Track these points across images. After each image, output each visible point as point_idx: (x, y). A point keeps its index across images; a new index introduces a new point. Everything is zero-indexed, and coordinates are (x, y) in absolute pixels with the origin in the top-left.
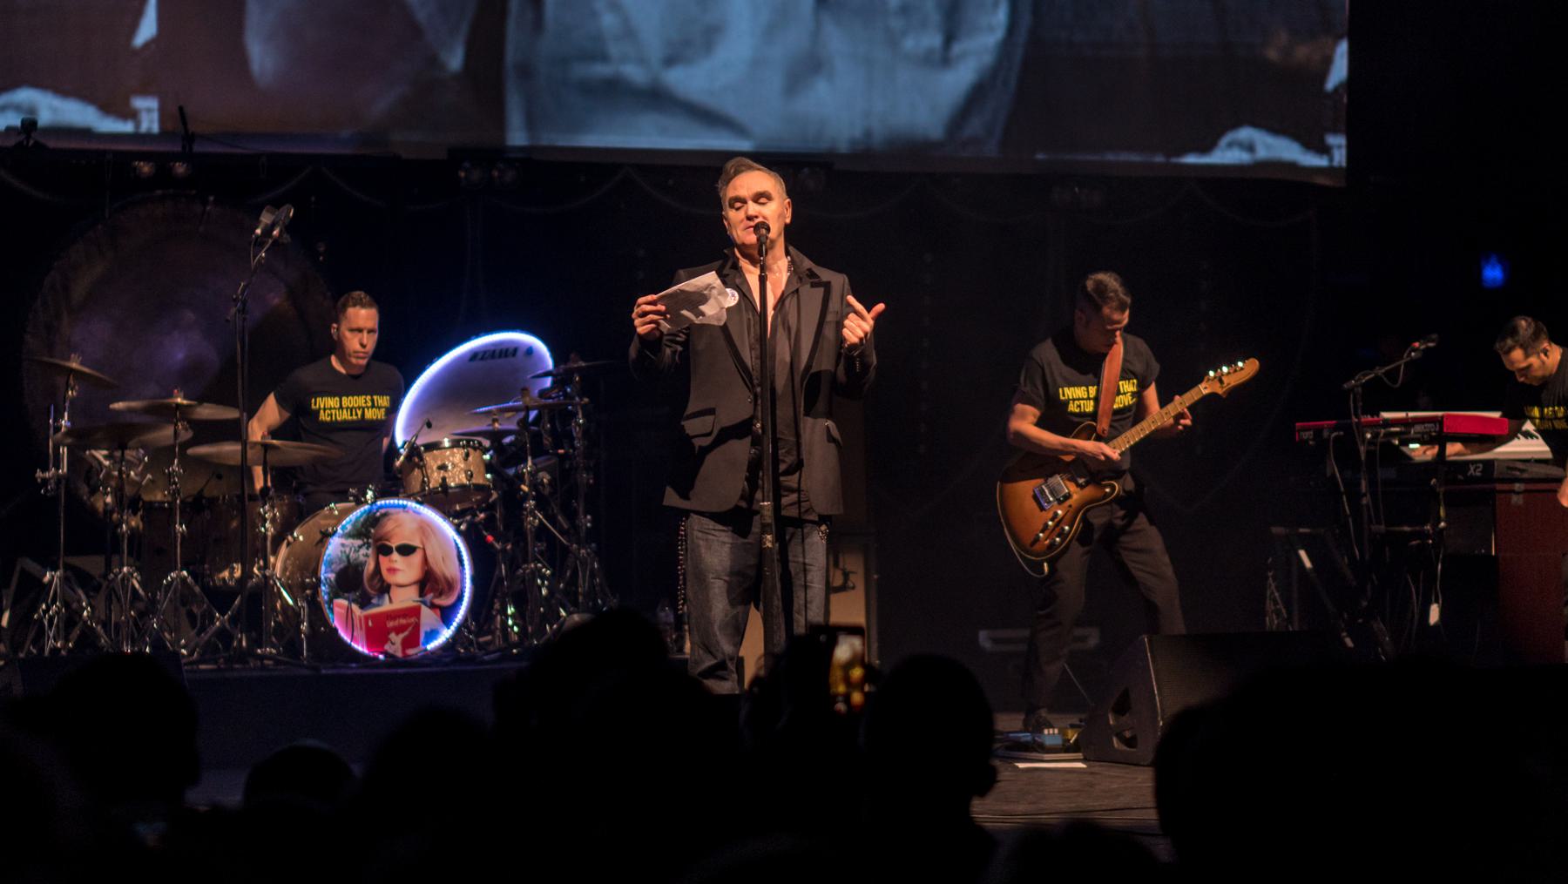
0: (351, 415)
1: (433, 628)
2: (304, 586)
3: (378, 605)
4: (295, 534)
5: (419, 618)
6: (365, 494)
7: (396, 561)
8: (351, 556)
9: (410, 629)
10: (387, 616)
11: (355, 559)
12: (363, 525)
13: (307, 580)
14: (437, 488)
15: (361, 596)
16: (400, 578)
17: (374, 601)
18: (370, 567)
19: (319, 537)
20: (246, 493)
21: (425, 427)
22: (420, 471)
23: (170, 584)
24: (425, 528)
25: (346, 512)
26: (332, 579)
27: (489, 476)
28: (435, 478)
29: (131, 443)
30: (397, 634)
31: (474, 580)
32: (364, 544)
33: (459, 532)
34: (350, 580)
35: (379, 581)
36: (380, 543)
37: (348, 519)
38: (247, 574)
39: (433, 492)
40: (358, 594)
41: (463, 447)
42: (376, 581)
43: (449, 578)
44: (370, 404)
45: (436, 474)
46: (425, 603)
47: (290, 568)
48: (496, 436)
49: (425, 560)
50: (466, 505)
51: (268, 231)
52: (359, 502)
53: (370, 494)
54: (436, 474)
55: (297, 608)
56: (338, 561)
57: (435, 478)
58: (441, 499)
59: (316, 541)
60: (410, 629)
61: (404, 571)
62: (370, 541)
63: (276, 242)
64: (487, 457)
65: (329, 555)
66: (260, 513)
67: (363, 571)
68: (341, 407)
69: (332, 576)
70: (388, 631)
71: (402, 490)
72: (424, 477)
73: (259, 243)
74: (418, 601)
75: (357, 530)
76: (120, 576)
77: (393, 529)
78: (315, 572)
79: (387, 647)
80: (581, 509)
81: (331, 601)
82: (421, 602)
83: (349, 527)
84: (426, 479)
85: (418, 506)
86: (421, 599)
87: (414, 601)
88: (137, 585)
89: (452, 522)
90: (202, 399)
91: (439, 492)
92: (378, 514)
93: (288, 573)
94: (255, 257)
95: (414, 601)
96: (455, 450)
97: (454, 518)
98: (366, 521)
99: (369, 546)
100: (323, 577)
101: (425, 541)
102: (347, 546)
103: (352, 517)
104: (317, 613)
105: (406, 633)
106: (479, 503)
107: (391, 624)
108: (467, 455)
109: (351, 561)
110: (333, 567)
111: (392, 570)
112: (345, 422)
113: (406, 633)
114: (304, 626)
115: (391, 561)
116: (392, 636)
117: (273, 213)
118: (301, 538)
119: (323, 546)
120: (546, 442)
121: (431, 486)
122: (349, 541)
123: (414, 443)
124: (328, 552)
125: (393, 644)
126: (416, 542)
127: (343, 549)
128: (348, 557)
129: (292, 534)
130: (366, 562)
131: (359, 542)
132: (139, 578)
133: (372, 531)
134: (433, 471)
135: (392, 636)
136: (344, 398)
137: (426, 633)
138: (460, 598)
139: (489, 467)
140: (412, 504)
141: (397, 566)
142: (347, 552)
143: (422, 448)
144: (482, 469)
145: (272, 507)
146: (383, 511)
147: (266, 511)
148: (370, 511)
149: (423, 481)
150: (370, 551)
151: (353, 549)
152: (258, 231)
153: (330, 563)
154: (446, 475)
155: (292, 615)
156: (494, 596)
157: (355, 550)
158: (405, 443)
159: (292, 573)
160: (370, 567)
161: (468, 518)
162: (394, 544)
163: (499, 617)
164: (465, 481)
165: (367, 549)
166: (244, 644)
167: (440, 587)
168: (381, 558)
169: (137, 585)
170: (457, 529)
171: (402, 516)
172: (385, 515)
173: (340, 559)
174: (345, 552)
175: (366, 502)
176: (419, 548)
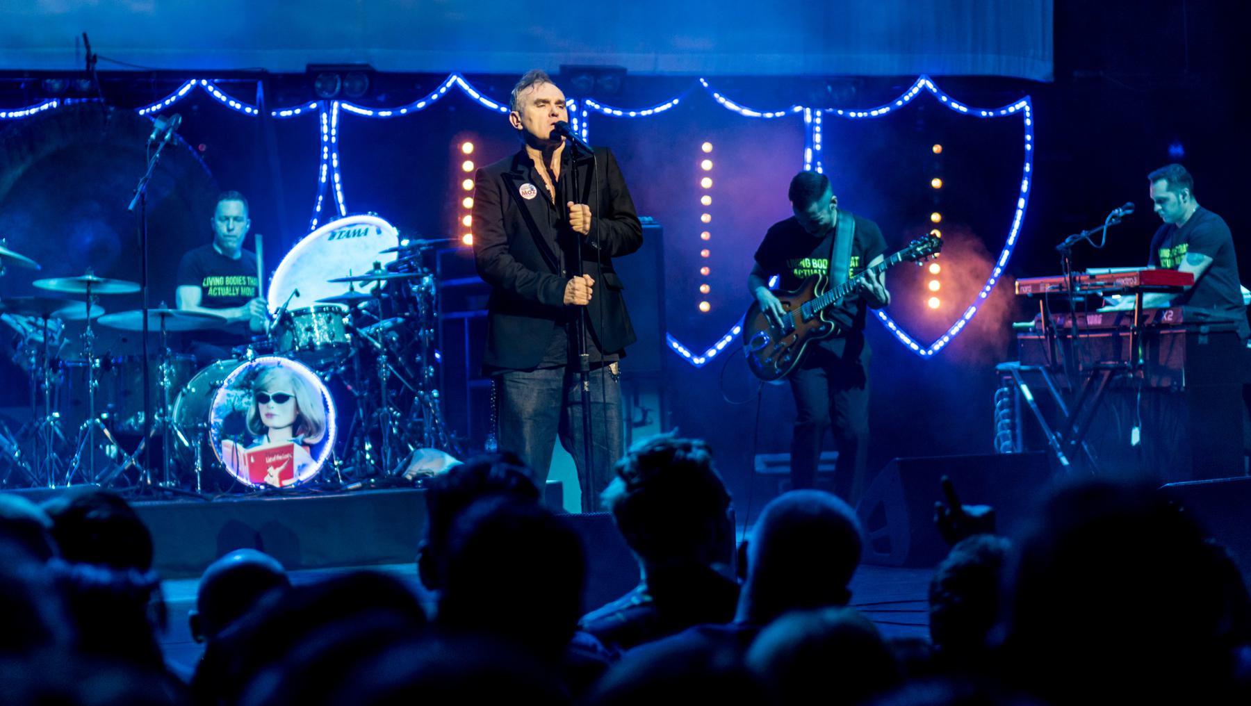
0: (232, 292)
1: (304, 462)
2: (196, 430)
3: (259, 444)
4: (189, 387)
5: (292, 455)
6: (245, 352)
8: (236, 403)
9: (286, 463)
11: (239, 407)
12: (245, 378)
13: (200, 425)
14: (305, 346)
15: (244, 437)
17: (255, 441)
18: (251, 413)
19: (208, 388)
20: (148, 353)
21: (295, 296)
22: (291, 333)
23: (86, 430)
24: (296, 379)
25: (230, 368)
26: (220, 423)
27: (348, 336)
28: (304, 338)
29: (54, 314)
30: (275, 468)
31: (338, 421)
32: (246, 394)
33: (324, 382)
34: (237, 426)
35: (259, 424)
36: (258, 393)
37: (232, 374)
38: (149, 421)
39: (302, 350)
40: (241, 435)
41: (326, 312)
42: (256, 425)
43: (318, 422)
44: (245, 283)
45: (304, 335)
46: (297, 442)
47: (184, 415)
48: (352, 301)
49: (297, 407)
50: (330, 360)
51: (161, 135)
52: (241, 358)
53: (250, 353)
54: (304, 335)
55: (191, 449)
56: (225, 408)
57: (304, 338)
58: (308, 355)
59: (206, 392)
60: (286, 463)
61: (281, 416)
62: (251, 391)
63: (168, 145)
64: (346, 320)
65: (218, 404)
66: (159, 370)
69: (220, 421)
70: (267, 466)
71: (276, 349)
72: (294, 336)
73: (154, 145)
75: (240, 382)
76: (44, 424)
77: (270, 381)
78: (206, 418)
79: (267, 479)
80: (425, 363)
81: (219, 442)
82: (294, 441)
83: (233, 380)
84: (295, 339)
85: (290, 361)
86: (294, 439)
87: (288, 441)
88: (58, 431)
89: (318, 375)
90: (110, 275)
91: (307, 350)
92: (257, 369)
93: (183, 419)
94: (151, 158)
95: (288, 441)
96: (320, 315)
97: (321, 370)
98: (247, 375)
99: (250, 395)
100: (212, 422)
101: (295, 389)
103: (237, 371)
104: (209, 455)
105: (282, 467)
106: (340, 358)
108: (330, 318)
109: (236, 408)
110: (221, 413)
111: (269, 415)
112: (227, 297)
113: (282, 467)
114: (198, 463)
115: (268, 407)
116: (271, 470)
117: (164, 120)
118: (193, 390)
119: (212, 397)
120: (393, 306)
121: (300, 345)
122: (234, 392)
123: (285, 310)
124: (216, 401)
125: (271, 476)
126: (288, 392)
127: (229, 399)
129: (186, 386)
130: (248, 408)
131: (242, 392)
132: (60, 425)
133: (253, 383)
134: (301, 333)
135: (271, 470)
137: (299, 467)
138: (326, 437)
139: (348, 329)
140: (284, 361)
141: (272, 411)
142: (232, 399)
143: (292, 314)
144: (342, 330)
145: (169, 364)
146: (261, 366)
147: (164, 367)
148: (251, 366)
149: (294, 341)
150: (251, 400)
151: (237, 398)
152: (153, 136)
153: (218, 410)
154: (313, 336)
155: (189, 454)
156: (354, 434)
158: (278, 310)
159: (186, 419)
160: (251, 413)
161: (332, 370)
162: (270, 394)
163: (358, 452)
164: (328, 340)
165: (249, 398)
166: (149, 481)
167: (310, 429)
168: (261, 405)
169: (58, 431)
170: (322, 378)
171: (277, 370)
172: (263, 370)
173: (226, 407)
174: (230, 400)
175: (247, 359)
176: (291, 396)
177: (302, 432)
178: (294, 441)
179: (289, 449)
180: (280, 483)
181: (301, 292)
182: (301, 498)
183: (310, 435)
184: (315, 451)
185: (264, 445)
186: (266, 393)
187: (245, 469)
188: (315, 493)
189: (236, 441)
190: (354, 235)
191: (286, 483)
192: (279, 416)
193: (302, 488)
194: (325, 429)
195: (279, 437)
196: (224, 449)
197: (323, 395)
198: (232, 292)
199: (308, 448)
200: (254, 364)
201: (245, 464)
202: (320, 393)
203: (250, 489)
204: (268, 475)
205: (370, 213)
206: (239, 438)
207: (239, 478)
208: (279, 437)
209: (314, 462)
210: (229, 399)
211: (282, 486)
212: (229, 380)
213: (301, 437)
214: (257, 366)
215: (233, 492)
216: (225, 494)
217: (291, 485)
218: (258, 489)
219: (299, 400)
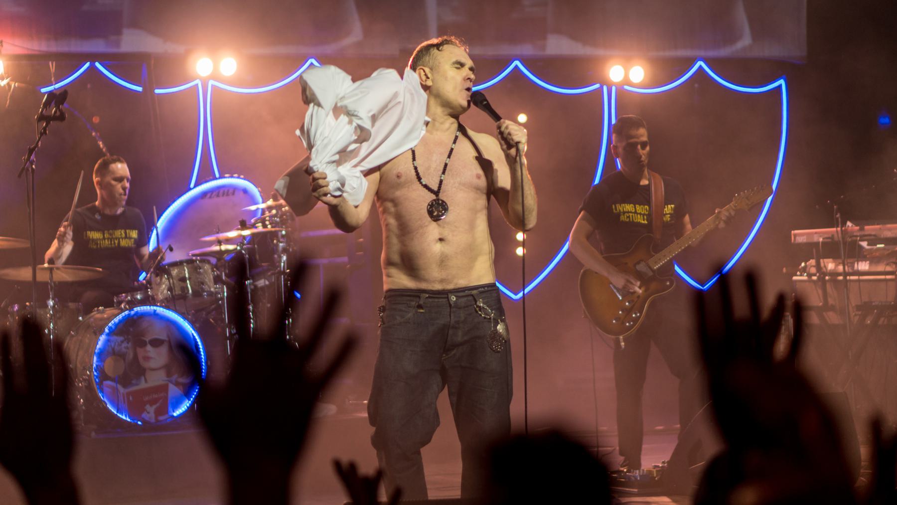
3: (137, 385)
5: (167, 393)
7: (149, 351)
8: (116, 347)
16: (152, 364)
21: (168, 250)
30: (151, 405)
37: (113, 322)
46: (171, 382)
60: (161, 401)
62: (130, 337)
65: (99, 349)
74: (166, 380)
79: (145, 415)
81: (100, 384)
82: (168, 380)
87: (163, 380)
95: (163, 380)
105: (158, 405)
107: (146, 398)
111: (147, 358)
113: (158, 405)
116: (148, 407)
122: (115, 338)
125: (148, 413)
130: (127, 352)
131: (122, 338)
133: (131, 329)
135: (148, 407)
140: (160, 310)
142: (113, 345)
148: (129, 314)
150: (130, 345)
151: (117, 344)
160: (131, 356)
165: (128, 343)
178: (169, 381)
179: (164, 388)
190: (223, 194)
191: (161, 418)
196: (106, 389)
198: (111, 244)
200: (133, 313)
201: (125, 402)
202: (192, 336)
204: (145, 412)
205: (236, 175)
211: (157, 421)
212: (110, 328)
214: (134, 315)
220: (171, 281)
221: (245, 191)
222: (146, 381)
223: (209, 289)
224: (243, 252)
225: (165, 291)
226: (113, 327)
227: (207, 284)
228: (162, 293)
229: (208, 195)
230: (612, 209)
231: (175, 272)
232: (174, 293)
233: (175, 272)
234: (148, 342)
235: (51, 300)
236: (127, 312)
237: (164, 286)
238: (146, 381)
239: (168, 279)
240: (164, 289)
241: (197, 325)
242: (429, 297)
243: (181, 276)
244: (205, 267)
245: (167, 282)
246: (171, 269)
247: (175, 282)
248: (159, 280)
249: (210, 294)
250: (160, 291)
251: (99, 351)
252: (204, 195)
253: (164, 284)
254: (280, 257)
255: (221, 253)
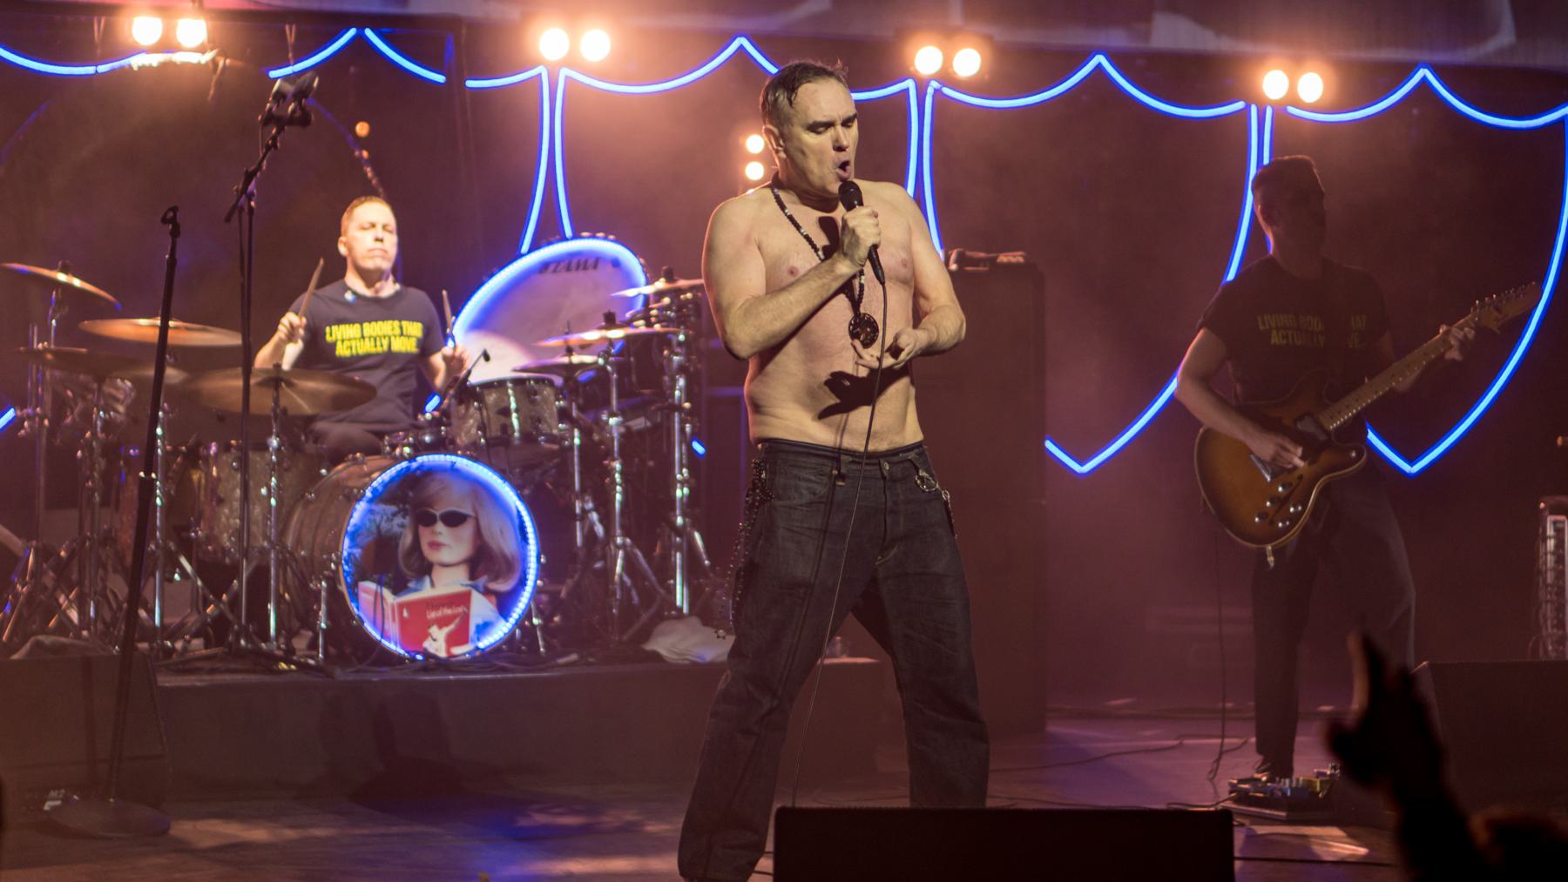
1: (487, 619)
3: (416, 590)
5: (468, 607)
7: (440, 533)
9: (457, 621)
10: (428, 603)
11: (389, 530)
16: (445, 556)
17: (411, 585)
21: (482, 359)
26: (357, 555)
30: (440, 627)
32: (399, 512)
37: (380, 480)
40: (390, 575)
46: (476, 588)
49: (478, 533)
60: (457, 621)
62: (407, 506)
65: (355, 525)
67: (397, 545)
68: (363, 337)
69: (357, 552)
70: (429, 624)
74: (467, 585)
79: (429, 645)
81: (353, 588)
85: (470, 463)
87: (462, 585)
92: (419, 472)
99: (404, 513)
102: (378, 513)
105: (452, 627)
109: (383, 531)
111: (436, 546)
113: (452, 627)
115: (434, 533)
116: (434, 630)
122: (380, 507)
125: (435, 640)
128: (378, 527)
130: (401, 533)
131: (393, 508)
133: (411, 494)
135: (434, 630)
136: (366, 325)
138: (522, 582)
141: (441, 539)
142: (378, 518)
148: (408, 468)
150: (407, 521)
151: (385, 518)
157: (388, 518)
160: (407, 539)
174: (375, 521)
177: (484, 574)
179: (462, 599)
180: (448, 651)
181: (489, 352)
182: (478, 677)
183: (496, 577)
184: (504, 604)
185: (426, 591)
186: (432, 511)
187: (393, 628)
188: (504, 670)
189: (380, 583)
190: (577, 268)
191: (457, 650)
192: (449, 546)
193: (486, 659)
194: (520, 568)
195: (449, 581)
196: (363, 596)
197: (520, 517)
199: (494, 599)
200: (414, 465)
201: (394, 620)
203: (400, 659)
204: (430, 638)
205: (601, 234)
206: (385, 579)
207: (385, 642)
208: (449, 581)
209: (502, 622)
210: (372, 517)
211: (451, 656)
212: (375, 490)
213: (482, 581)
214: (418, 468)
215: (374, 664)
216: (359, 667)
217: (464, 654)
218: (413, 660)
219: (483, 523)
220: (485, 413)
221: (616, 263)
222: (433, 584)
223: (549, 431)
224: (609, 368)
225: (473, 431)
226: (380, 488)
227: (546, 422)
228: (469, 431)
229: (552, 268)
230: (325, 334)
231: (491, 398)
232: (488, 435)
233: (491, 398)
234: (438, 518)
235: (273, 437)
236: (404, 464)
237: (471, 421)
238: (433, 584)
239: (480, 409)
240: (472, 426)
241: (527, 492)
242: (853, 462)
243: (503, 405)
244: (545, 392)
245: (477, 415)
246: (486, 392)
247: (492, 415)
248: (463, 411)
249: (552, 439)
250: (465, 429)
251: (353, 529)
252: (544, 266)
253: (471, 417)
254: (674, 381)
255: (571, 368)
